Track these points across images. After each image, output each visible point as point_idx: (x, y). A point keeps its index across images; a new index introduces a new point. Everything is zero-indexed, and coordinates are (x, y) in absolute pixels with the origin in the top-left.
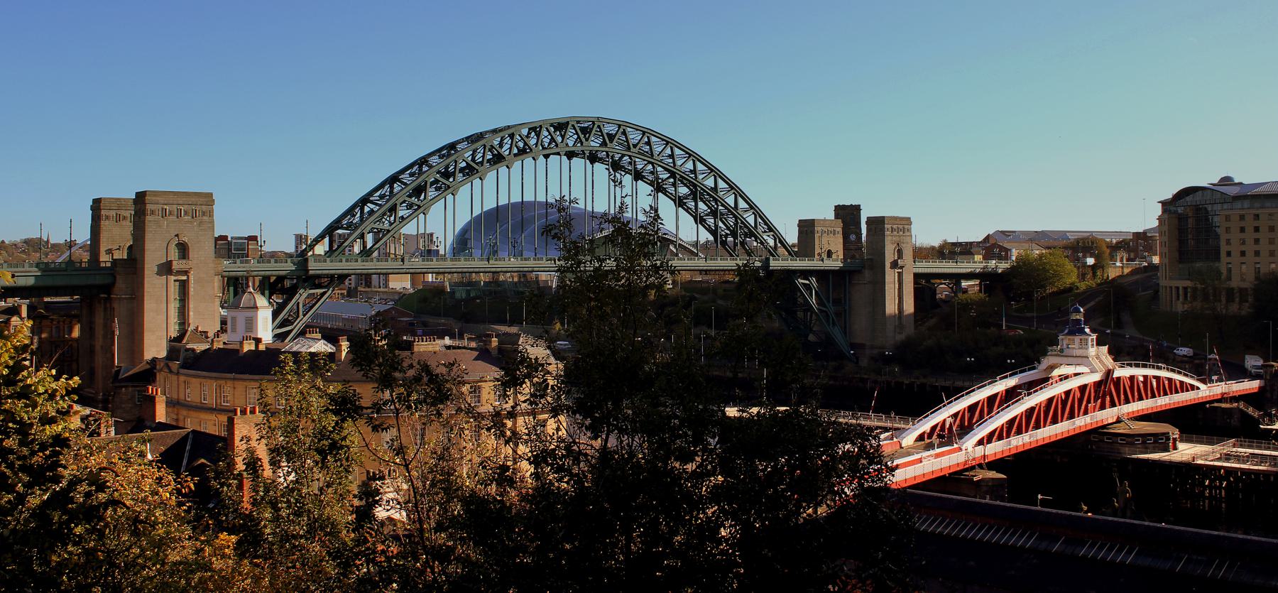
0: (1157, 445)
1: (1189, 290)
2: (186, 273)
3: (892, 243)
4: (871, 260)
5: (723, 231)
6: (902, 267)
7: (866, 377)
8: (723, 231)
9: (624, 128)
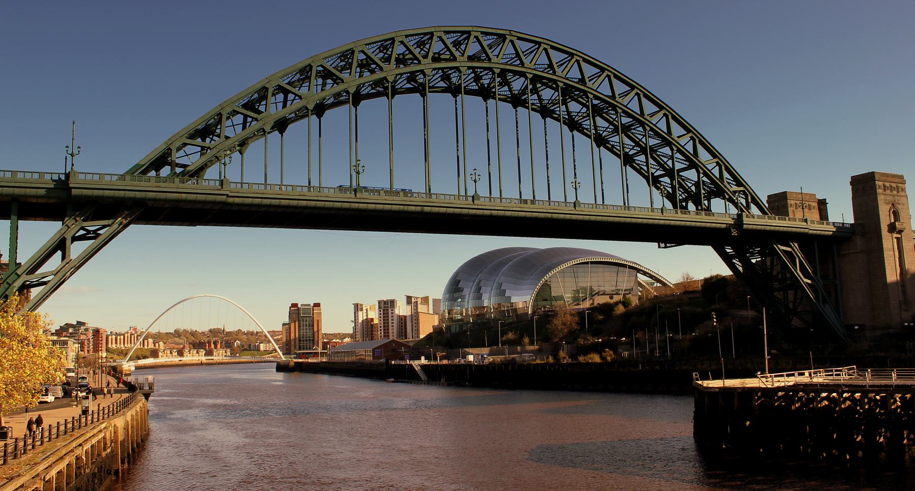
3: (887, 204)
6: (900, 232)
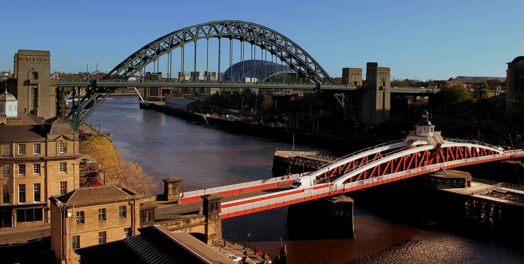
0: (458, 184)
1: (514, 104)
2: (36, 85)
3: (380, 79)
4: (371, 86)
5: (302, 72)
7: (360, 138)
8: (302, 72)
9: (251, 25)
